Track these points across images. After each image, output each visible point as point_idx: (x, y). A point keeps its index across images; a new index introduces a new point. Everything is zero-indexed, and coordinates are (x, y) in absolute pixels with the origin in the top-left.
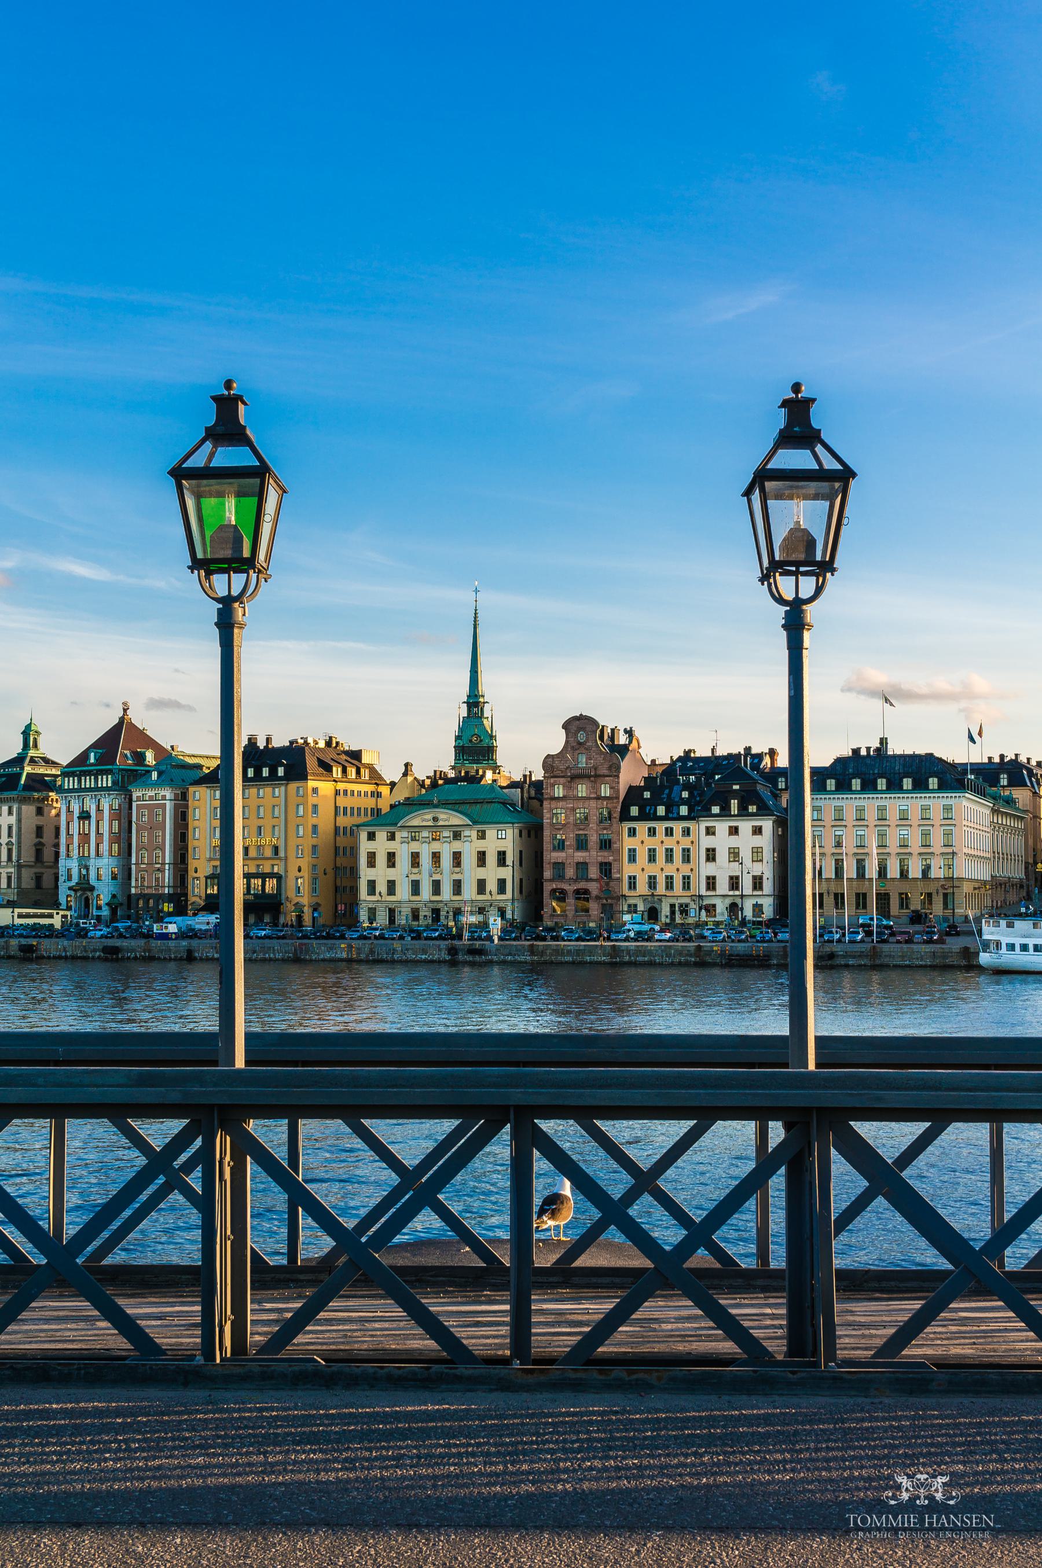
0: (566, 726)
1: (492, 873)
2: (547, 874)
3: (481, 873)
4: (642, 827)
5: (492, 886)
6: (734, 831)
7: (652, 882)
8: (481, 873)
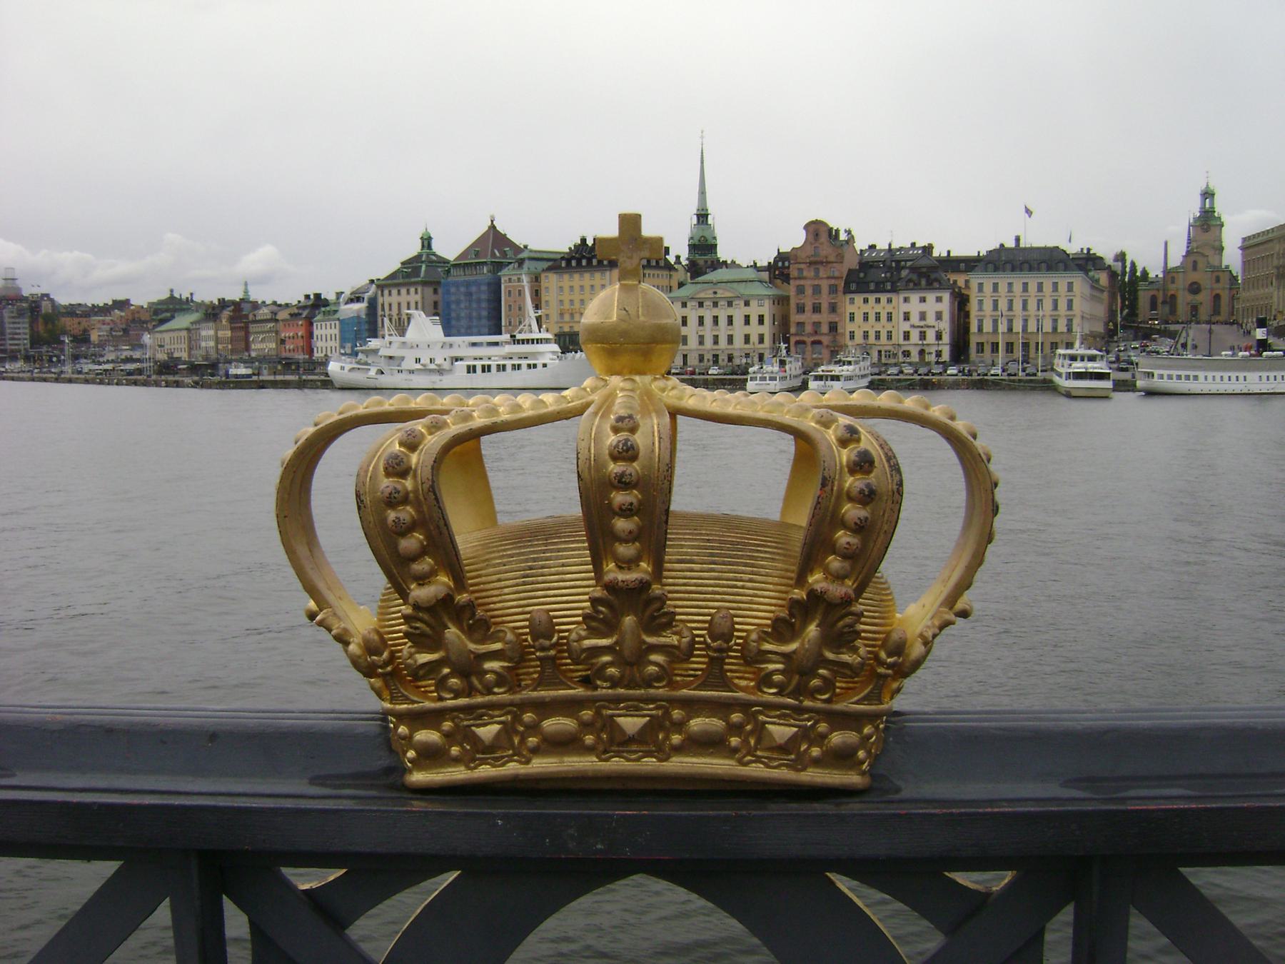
0: (807, 227)
1: (754, 330)
2: (793, 330)
3: (747, 330)
4: (859, 298)
5: (754, 338)
6: (923, 300)
7: (866, 335)
8: (747, 330)
